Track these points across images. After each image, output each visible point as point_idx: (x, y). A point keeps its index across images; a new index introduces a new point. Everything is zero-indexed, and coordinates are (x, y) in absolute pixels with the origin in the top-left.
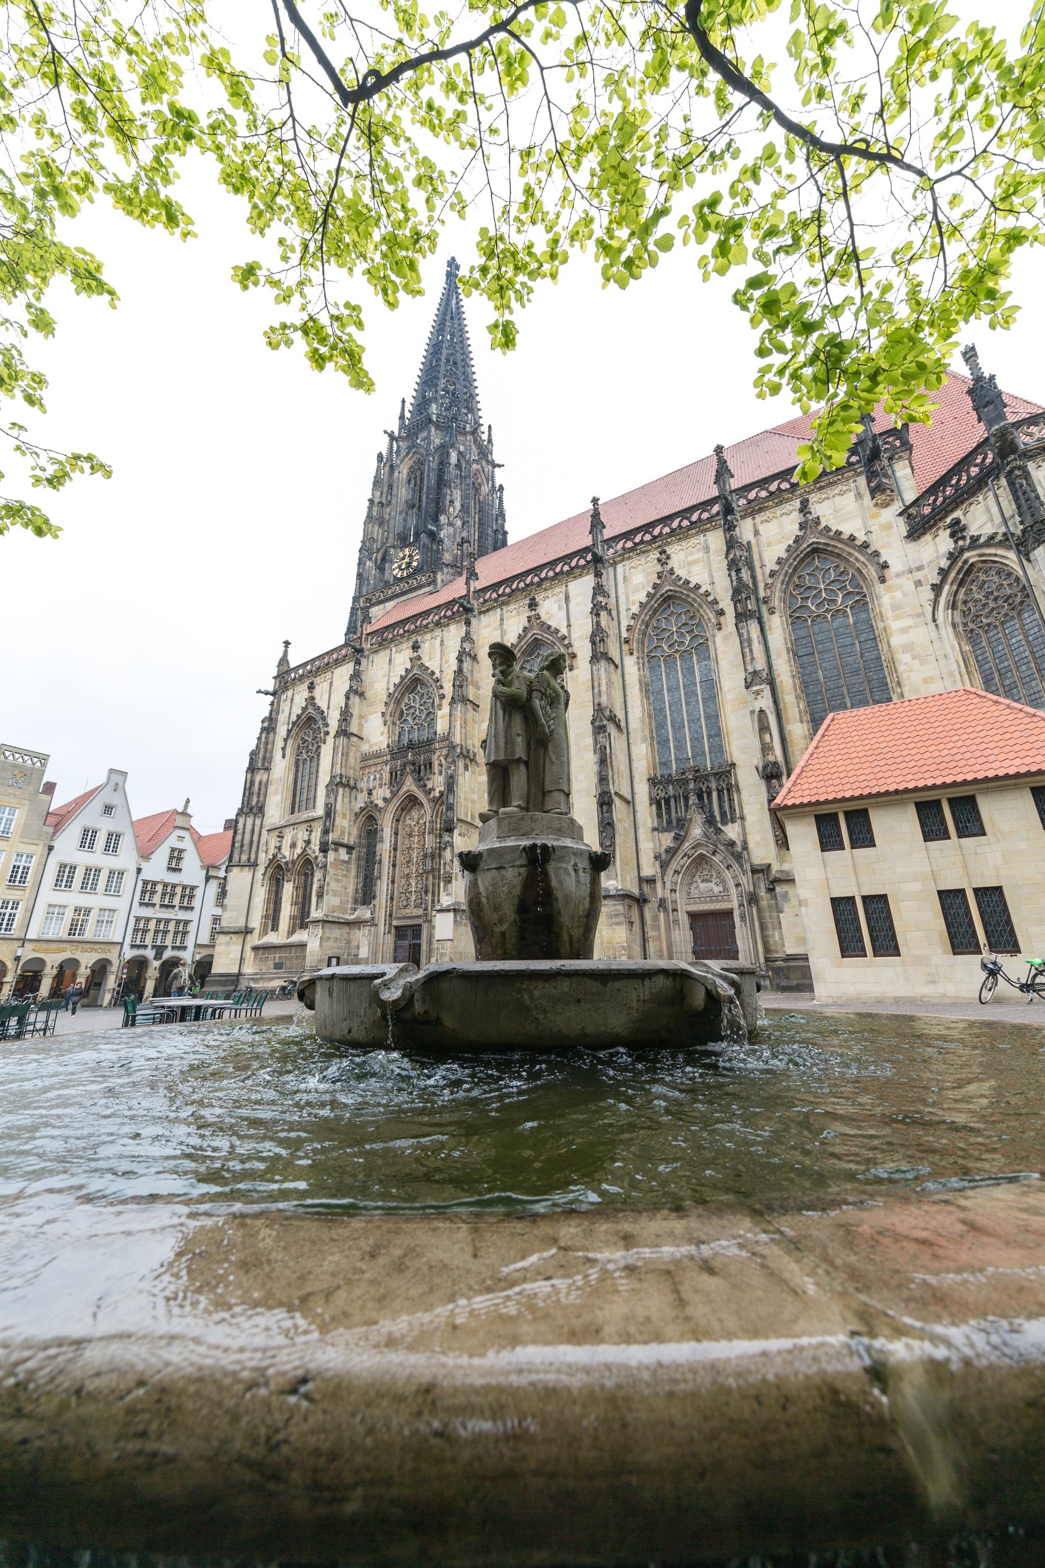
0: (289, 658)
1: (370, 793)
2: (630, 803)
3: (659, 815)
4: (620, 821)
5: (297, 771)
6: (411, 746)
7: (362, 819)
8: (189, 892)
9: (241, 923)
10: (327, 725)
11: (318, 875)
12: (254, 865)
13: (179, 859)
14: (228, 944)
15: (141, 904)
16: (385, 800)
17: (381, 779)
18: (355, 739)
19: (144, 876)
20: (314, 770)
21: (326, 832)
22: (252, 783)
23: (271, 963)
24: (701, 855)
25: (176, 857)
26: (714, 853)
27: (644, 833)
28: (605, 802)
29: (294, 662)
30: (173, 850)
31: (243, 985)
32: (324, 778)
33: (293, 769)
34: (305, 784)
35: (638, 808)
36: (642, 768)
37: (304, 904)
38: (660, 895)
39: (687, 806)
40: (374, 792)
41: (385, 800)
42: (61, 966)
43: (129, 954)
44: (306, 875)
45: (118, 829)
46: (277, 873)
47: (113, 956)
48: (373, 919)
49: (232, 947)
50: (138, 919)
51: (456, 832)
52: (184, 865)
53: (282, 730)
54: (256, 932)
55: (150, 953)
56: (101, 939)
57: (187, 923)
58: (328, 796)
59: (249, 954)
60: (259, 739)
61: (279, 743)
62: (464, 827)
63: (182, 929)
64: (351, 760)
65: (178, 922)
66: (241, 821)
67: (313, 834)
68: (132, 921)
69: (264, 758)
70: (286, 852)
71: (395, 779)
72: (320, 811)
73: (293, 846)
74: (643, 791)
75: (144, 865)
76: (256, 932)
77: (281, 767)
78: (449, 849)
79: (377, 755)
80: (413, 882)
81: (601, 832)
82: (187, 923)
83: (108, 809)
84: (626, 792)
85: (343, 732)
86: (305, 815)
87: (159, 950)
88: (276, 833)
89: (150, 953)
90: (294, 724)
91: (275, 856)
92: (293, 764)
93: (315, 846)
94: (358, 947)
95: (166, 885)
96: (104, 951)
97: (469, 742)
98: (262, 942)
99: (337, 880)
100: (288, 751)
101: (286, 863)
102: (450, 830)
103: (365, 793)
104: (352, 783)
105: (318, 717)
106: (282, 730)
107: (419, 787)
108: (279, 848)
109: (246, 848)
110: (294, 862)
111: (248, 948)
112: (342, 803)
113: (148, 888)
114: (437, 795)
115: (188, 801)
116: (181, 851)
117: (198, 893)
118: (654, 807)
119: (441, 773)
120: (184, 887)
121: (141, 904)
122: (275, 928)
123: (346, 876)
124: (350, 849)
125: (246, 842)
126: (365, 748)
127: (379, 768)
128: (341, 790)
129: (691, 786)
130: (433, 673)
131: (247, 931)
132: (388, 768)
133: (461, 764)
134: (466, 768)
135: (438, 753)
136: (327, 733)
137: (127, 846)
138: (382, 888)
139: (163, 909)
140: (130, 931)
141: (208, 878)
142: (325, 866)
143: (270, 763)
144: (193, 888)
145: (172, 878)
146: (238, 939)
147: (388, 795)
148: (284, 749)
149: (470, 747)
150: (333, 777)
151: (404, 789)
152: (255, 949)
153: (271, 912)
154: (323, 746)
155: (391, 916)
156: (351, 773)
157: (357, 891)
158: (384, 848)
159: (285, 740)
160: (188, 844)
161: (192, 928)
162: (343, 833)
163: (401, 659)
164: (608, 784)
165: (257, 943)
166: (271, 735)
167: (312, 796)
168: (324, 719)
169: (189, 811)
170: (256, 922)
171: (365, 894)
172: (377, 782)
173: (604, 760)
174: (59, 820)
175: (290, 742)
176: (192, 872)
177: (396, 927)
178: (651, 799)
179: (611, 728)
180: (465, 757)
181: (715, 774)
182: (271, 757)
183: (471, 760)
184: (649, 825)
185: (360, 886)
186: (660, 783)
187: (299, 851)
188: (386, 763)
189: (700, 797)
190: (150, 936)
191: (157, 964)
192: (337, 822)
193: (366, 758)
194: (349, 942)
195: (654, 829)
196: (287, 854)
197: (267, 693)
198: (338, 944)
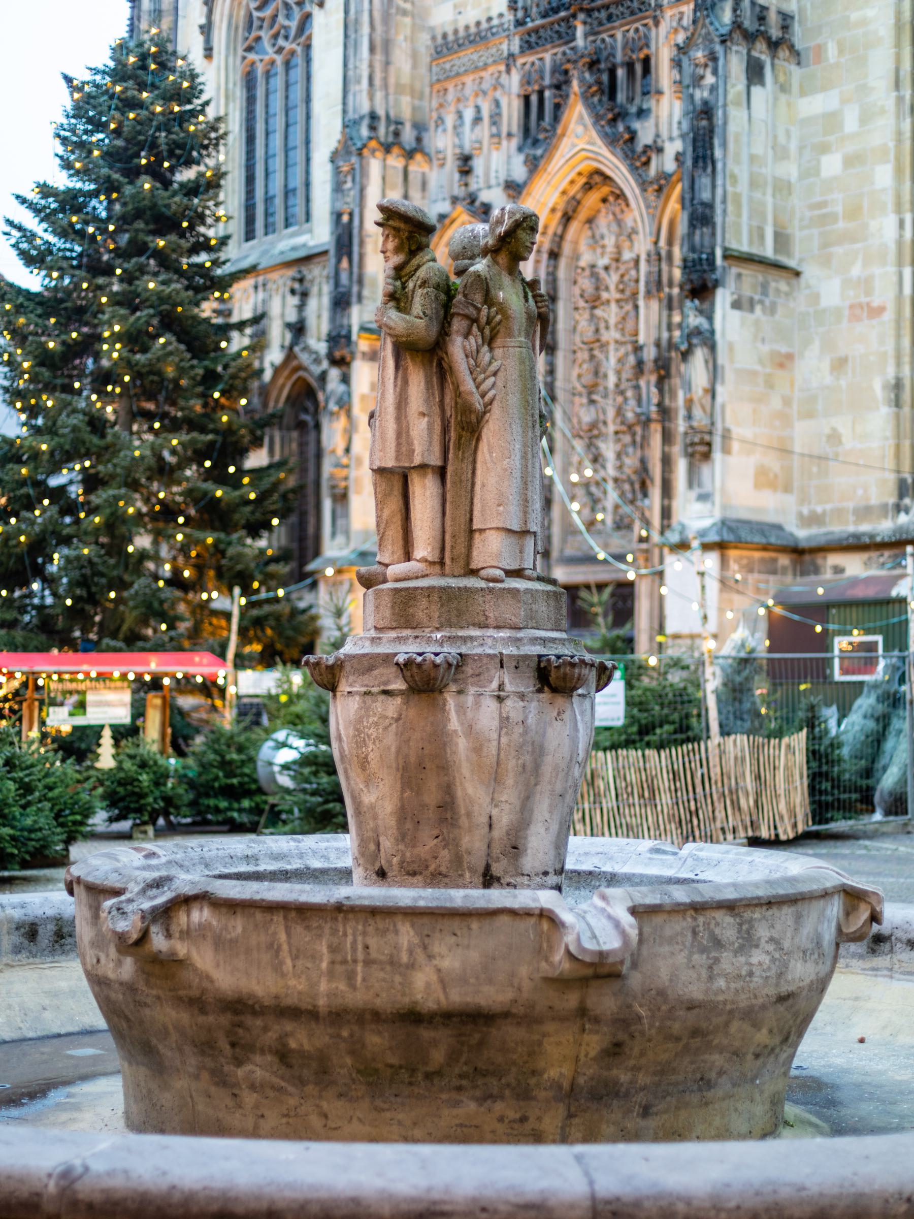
5: (251, 100)
20: (297, 93)
32: (327, 132)
34: (277, 140)
40: (478, 164)
51: (722, 298)
58: (338, 188)
62: (751, 276)
64: (402, 61)
78: (699, 355)
79: (477, 37)
86: (287, 243)
92: (237, 77)
102: (701, 288)
103: (452, 165)
104: (408, 135)
107: (612, 141)
132: (514, 81)
133: (735, 64)
134: (755, 73)
147: (519, 172)
148: (206, 30)
150: (348, 125)
156: (405, 108)
167: (297, 181)
180: (750, 37)
183: (774, 46)
193: (447, 46)
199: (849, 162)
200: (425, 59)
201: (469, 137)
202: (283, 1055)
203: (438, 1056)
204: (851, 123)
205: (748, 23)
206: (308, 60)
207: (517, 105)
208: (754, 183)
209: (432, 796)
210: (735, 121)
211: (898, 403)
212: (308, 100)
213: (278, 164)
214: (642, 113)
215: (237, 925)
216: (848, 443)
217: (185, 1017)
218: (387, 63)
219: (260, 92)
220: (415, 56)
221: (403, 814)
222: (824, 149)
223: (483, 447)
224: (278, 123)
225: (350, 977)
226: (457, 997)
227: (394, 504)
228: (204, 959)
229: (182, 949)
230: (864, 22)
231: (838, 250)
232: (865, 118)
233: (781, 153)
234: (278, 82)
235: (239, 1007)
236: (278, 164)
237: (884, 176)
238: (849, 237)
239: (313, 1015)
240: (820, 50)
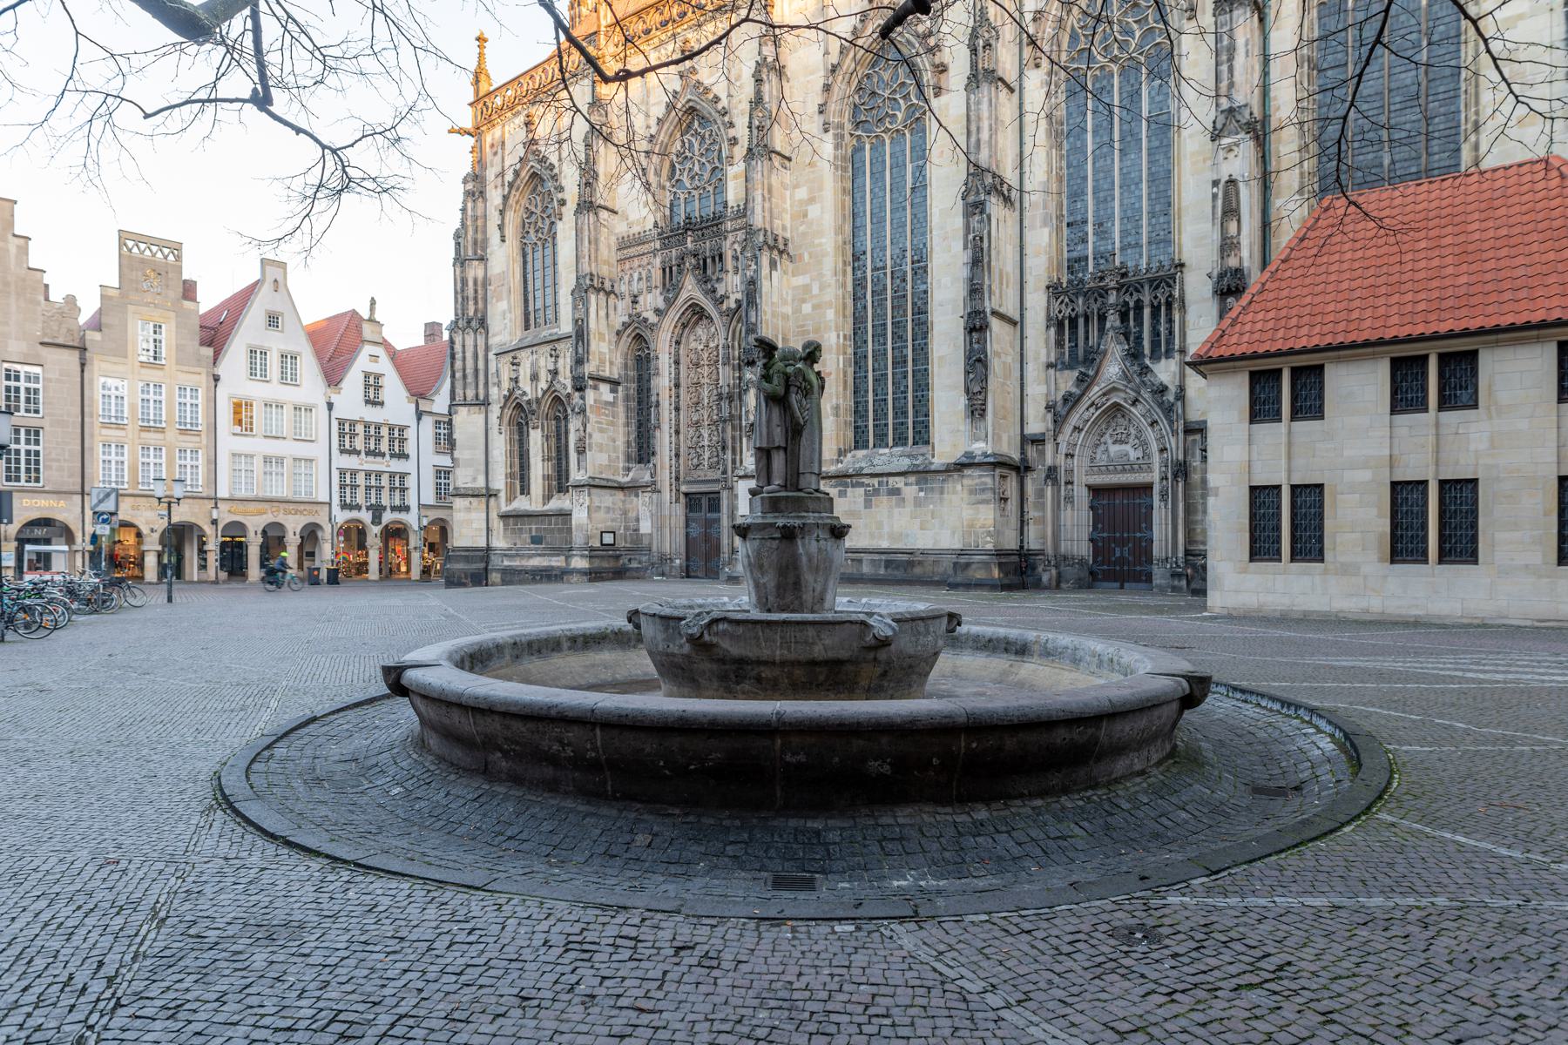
0: (490, 66)
1: (635, 302)
2: (1017, 323)
3: (1059, 344)
4: (998, 354)
5: (525, 263)
6: (689, 226)
7: (626, 340)
8: (398, 433)
9: (481, 483)
10: (561, 189)
11: (574, 424)
12: (485, 403)
13: (378, 387)
14: (468, 510)
15: (342, 452)
16: (658, 311)
17: (648, 279)
18: (604, 214)
19: (335, 414)
21: (579, 361)
22: (464, 282)
23: (526, 536)
24: (1116, 405)
25: (372, 384)
26: (1135, 402)
27: (1034, 370)
28: (976, 326)
29: (500, 73)
31: (496, 561)
33: (519, 259)
34: (539, 283)
35: (1029, 331)
36: (1040, 269)
37: (559, 460)
38: (1049, 461)
39: (1102, 330)
40: (641, 299)
41: (658, 311)
42: (264, 532)
43: (341, 517)
44: (557, 418)
45: (290, 347)
46: (520, 415)
47: (322, 519)
48: (654, 483)
49: (474, 515)
50: (342, 472)
52: (385, 395)
53: (495, 197)
54: (502, 495)
55: (366, 516)
56: (303, 497)
57: (403, 476)
58: (575, 308)
59: (497, 525)
60: (464, 210)
61: (494, 219)
63: (399, 483)
65: (392, 475)
66: (458, 339)
67: (561, 361)
68: (335, 475)
69: (475, 243)
70: (526, 385)
71: (670, 280)
72: (566, 327)
74: (1037, 303)
75: (335, 399)
76: (502, 495)
77: (503, 258)
79: (639, 240)
80: (705, 433)
81: (967, 373)
82: (403, 476)
83: (273, 320)
84: (1011, 309)
85: (587, 206)
86: (545, 333)
87: (377, 511)
88: (508, 358)
89: (366, 516)
90: (511, 185)
91: (511, 392)
93: (566, 379)
94: (638, 520)
95: (367, 426)
96: (310, 512)
97: (777, 223)
98: (510, 508)
99: (601, 430)
100: (510, 231)
101: (529, 402)
103: (628, 300)
104: (607, 286)
105: (546, 174)
106: (495, 197)
107: (706, 293)
108: (516, 380)
109: (470, 379)
110: (538, 401)
111: (494, 515)
112: (596, 324)
113: (346, 429)
114: (733, 306)
115: (373, 302)
116: (378, 377)
117: (410, 434)
118: (1053, 330)
119: (736, 270)
121: (342, 452)
122: (525, 490)
123: (612, 424)
124: (614, 384)
125: (470, 371)
126: (621, 228)
127: (645, 260)
128: (593, 298)
129: (1112, 298)
130: (717, 99)
131: (490, 494)
132: (658, 261)
134: (773, 265)
135: (731, 238)
136: (563, 203)
137: (309, 367)
138: (663, 441)
139: (371, 458)
140: (336, 488)
141: (419, 415)
142: (583, 411)
143: (484, 249)
144: (402, 429)
145: (373, 415)
146: (478, 504)
147: (661, 304)
148: (501, 227)
149: (779, 232)
151: (684, 295)
152: (504, 517)
153: (517, 469)
154: (560, 226)
155: (677, 479)
156: (605, 271)
157: (628, 443)
158: (662, 383)
159: (502, 212)
160: (385, 366)
161: (411, 482)
162: (602, 362)
164: (982, 299)
165: (504, 508)
166: (480, 204)
167: (549, 301)
168: (554, 178)
169: (377, 317)
170: (499, 482)
171: (640, 448)
172: (643, 285)
173: (979, 260)
174: (215, 334)
175: (510, 215)
176: (397, 406)
177: (686, 494)
178: (1049, 319)
179: (995, 206)
180: (771, 248)
181: (1151, 281)
182: (485, 240)
183: (781, 252)
184: (1043, 359)
185: (632, 437)
186: (1065, 293)
187: (543, 385)
188: (654, 252)
189: (1124, 317)
190: (361, 493)
191: (376, 530)
192: (593, 347)
193: (624, 244)
194: (625, 513)
195: (1050, 366)
196: (528, 389)
197: (463, 132)
198: (611, 515)
199: (815, 307)
200: (614, 248)
201: (635, 288)
202: (759, 679)
203: (822, 678)
204: (815, 290)
205: (771, 242)
206: (554, 245)
207: (660, 272)
208: (773, 315)
209: (791, 580)
210: (765, 286)
211: (837, 415)
212: (555, 264)
213: (539, 294)
214: (718, 280)
215: (741, 630)
217: (715, 667)
218: (597, 250)
219: (529, 258)
220: (609, 246)
221: (778, 587)
222: (804, 301)
223: (803, 439)
224: (539, 274)
225: (789, 649)
226: (831, 655)
227: (764, 461)
228: (725, 644)
229: (715, 640)
230: (820, 245)
232: (821, 289)
233: (785, 303)
234: (539, 255)
235: (741, 662)
236: (539, 294)
237: (830, 314)
239: (774, 663)
240: (801, 256)
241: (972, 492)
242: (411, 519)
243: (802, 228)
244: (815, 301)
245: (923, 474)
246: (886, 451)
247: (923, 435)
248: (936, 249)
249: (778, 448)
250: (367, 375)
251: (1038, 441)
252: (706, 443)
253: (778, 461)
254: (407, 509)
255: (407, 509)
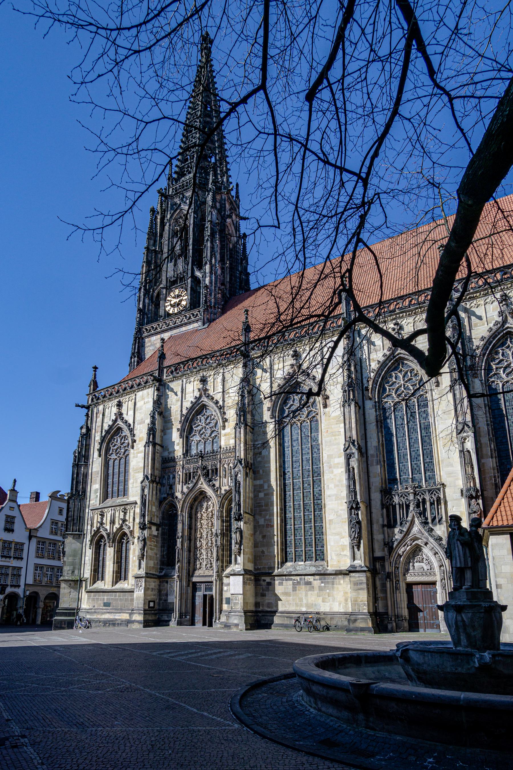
30: (7, 516)
65: (14, 568)
73: (113, 522)
91: (98, 529)
117: (26, 547)
120: (17, 544)
144: (22, 544)
163: (192, 388)
187: (117, 526)
196: (108, 527)
199: (265, 495)
216: (266, 553)
222: (260, 492)
231: (263, 513)
238: (265, 510)
241: (356, 584)
242: (20, 591)
243: (259, 459)
244: (266, 492)
245: (323, 574)
246: (303, 563)
247: (320, 555)
248: (326, 472)
249: (469, 568)
250: (7, 516)
251: (382, 559)
252: (205, 557)
253: (468, 575)
254: (19, 586)
255: (19, 586)
